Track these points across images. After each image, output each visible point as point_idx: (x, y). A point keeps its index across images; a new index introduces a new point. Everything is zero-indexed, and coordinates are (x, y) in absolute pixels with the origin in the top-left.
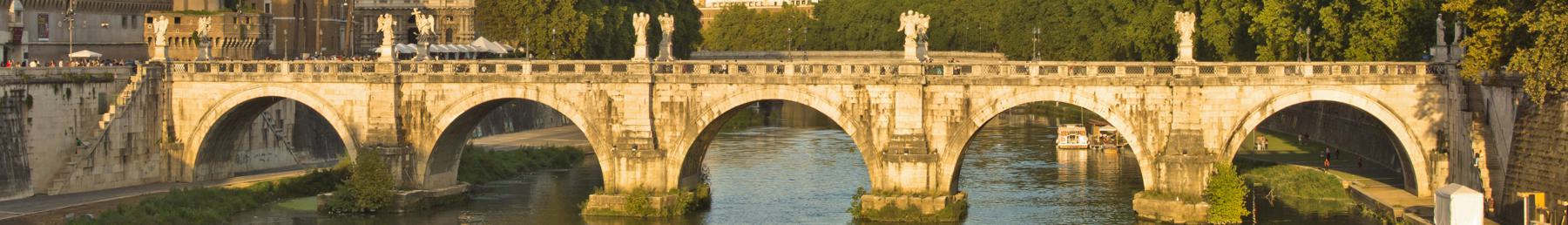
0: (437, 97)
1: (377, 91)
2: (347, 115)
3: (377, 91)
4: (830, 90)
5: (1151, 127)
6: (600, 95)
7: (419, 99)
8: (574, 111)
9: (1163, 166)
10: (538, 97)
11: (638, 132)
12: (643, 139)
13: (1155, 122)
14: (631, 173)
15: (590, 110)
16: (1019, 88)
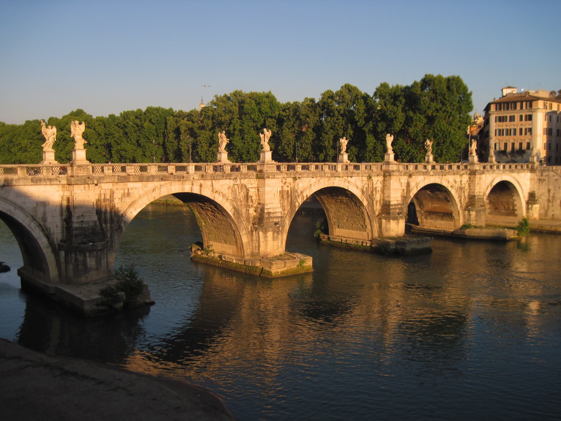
0: (124, 195)
1: (79, 192)
2: (40, 216)
3: (79, 192)
4: (357, 180)
5: (463, 194)
6: (241, 188)
7: (108, 197)
8: (225, 200)
9: (473, 213)
10: (200, 191)
11: (275, 213)
12: (278, 217)
13: (464, 192)
14: (276, 242)
15: (235, 199)
16: (426, 176)
